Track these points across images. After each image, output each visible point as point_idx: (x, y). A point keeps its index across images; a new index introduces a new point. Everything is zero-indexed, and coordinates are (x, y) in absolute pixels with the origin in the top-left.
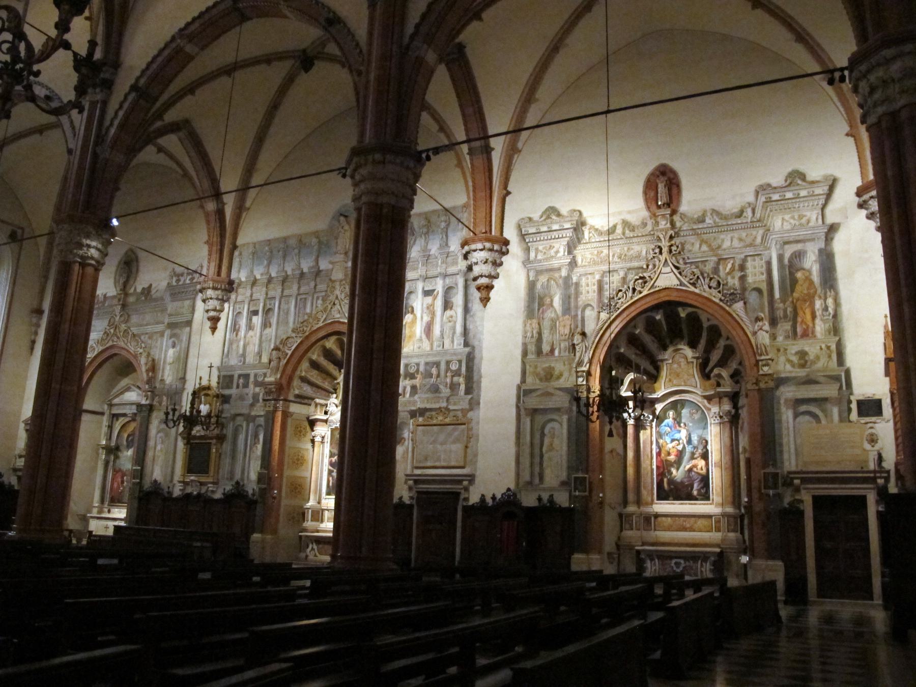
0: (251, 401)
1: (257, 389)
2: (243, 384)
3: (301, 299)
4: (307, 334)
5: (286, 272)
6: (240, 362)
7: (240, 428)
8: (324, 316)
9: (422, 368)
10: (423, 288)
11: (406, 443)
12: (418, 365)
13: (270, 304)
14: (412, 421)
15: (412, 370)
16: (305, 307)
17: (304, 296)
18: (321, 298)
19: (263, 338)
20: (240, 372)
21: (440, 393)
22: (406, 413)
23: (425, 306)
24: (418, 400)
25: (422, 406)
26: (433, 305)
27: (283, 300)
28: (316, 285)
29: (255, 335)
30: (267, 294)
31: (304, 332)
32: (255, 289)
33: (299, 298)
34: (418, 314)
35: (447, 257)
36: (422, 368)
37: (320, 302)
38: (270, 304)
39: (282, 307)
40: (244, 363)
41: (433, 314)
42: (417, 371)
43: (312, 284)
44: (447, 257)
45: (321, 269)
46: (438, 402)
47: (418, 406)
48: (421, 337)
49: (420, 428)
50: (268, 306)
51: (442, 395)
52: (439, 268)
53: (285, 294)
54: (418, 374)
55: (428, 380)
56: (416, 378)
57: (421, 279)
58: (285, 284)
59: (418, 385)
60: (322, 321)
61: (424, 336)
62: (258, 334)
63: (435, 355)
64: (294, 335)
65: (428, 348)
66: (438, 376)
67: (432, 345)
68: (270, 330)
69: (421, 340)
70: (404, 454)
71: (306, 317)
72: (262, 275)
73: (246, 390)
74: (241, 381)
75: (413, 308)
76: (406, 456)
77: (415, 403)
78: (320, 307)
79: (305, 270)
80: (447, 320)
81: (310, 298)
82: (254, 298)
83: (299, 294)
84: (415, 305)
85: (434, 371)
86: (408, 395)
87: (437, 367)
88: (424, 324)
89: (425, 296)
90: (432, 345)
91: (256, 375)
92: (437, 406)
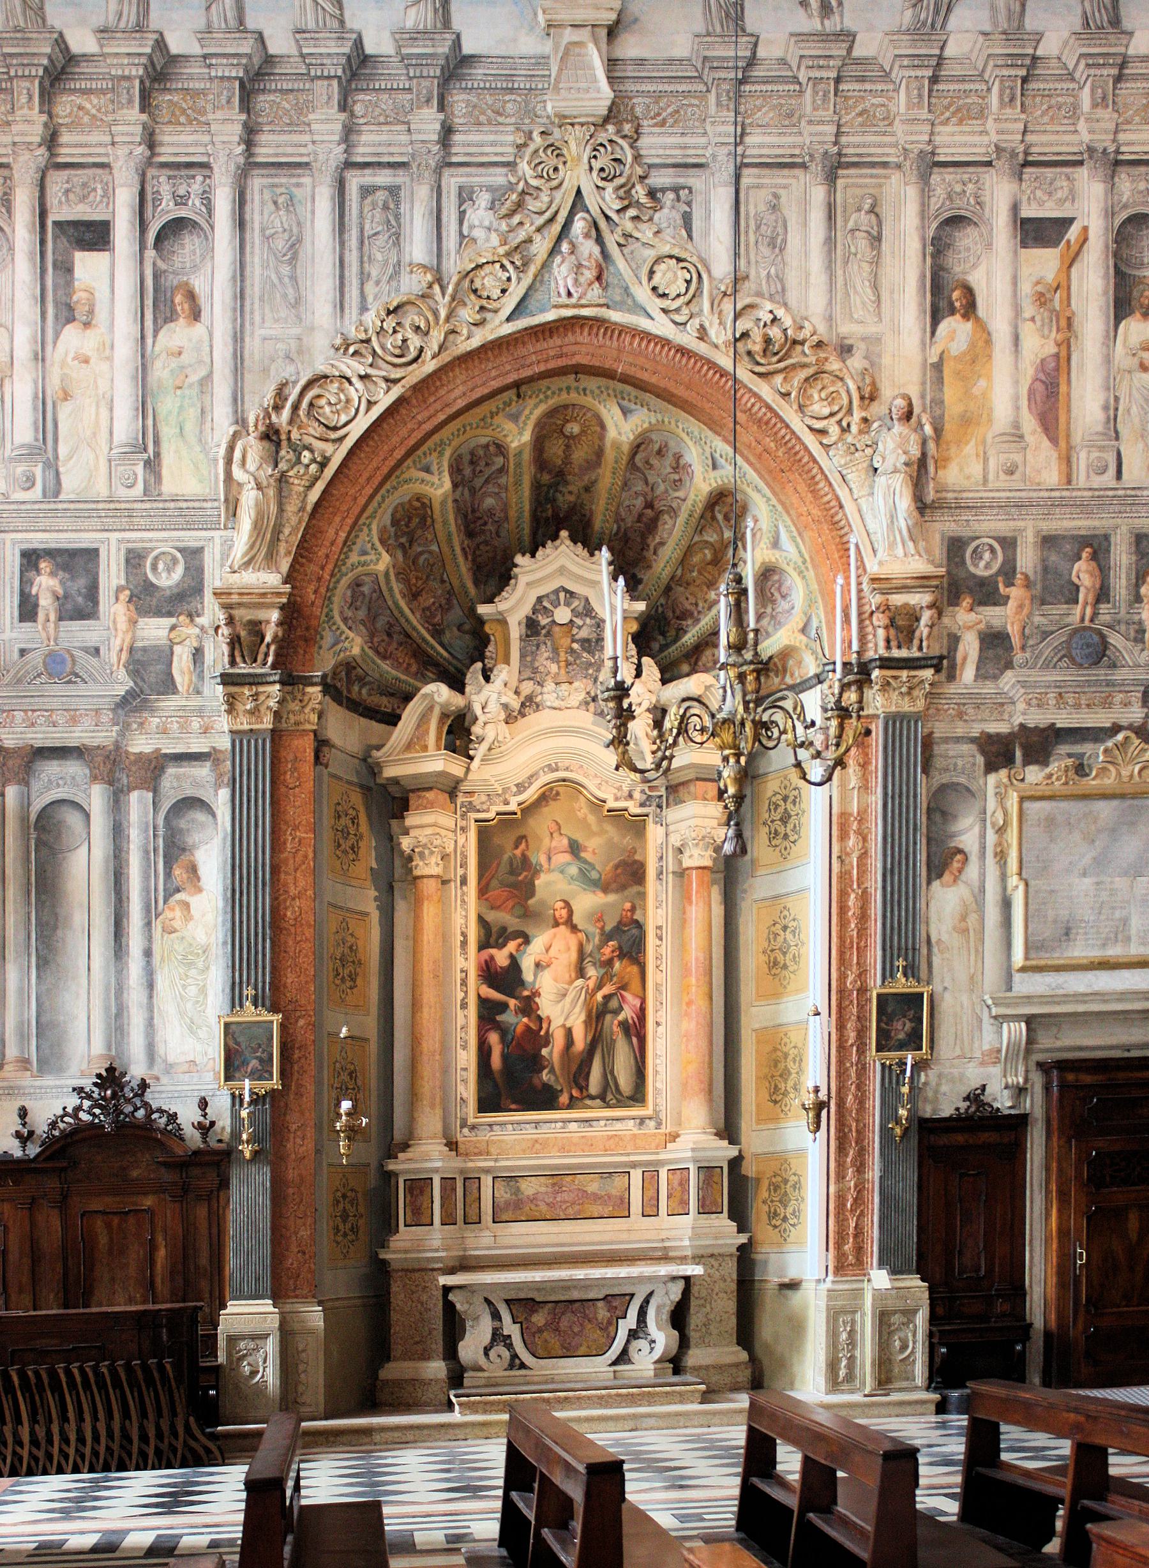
0: (123, 683)
1: (155, 630)
2: (62, 600)
3: (366, 191)
4: (429, 366)
5: (260, 38)
6: (30, 482)
7: (73, 819)
8: (516, 292)
9: (1027, 559)
10: (1015, 208)
11: (972, 871)
12: (1009, 543)
13: (181, 200)
14: (992, 779)
15: (983, 567)
16: (397, 239)
17: (383, 178)
18: (483, 199)
19: (160, 371)
20: (38, 540)
21: (1113, 666)
22: (967, 748)
23: (1026, 288)
24: (1018, 693)
25: (1037, 718)
26: (1063, 286)
27: (256, 183)
28: (447, 131)
29: (107, 349)
30: (151, 142)
31: (407, 358)
32: (65, 106)
33: (355, 181)
34: (1000, 325)
35: (1119, 79)
36: (1027, 559)
37: (479, 214)
38: (181, 200)
39: (256, 215)
40: (54, 489)
41: (1067, 325)
42: (1009, 572)
43: (428, 122)
44: (1119, 79)
45: (467, 49)
46: (1107, 703)
47: (1018, 720)
48: (1016, 425)
49: (1033, 807)
50: (166, 210)
51: (1120, 675)
52: (1082, 126)
53: (264, 153)
54: (1010, 584)
55: (1058, 610)
56: (1003, 601)
57: (1001, 164)
58: (262, 101)
59: (1013, 630)
60: (509, 304)
61: (1030, 424)
62: (124, 350)
63: (1084, 508)
64: (353, 367)
65: (1052, 476)
66: (1103, 594)
67: (1067, 461)
68: (199, 329)
69: (1017, 436)
70: (963, 918)
71: (412, 284)
72: (103, 32)
73: (79, 633)
74: (46, 584)
75: (969, 292)
76: (973, 919)
77: (1001, 705)
78: (489, 244)
79: (377, 43)
80: (1133, 363)
81: (423, 192)
82: (66, 154)
83: (349, 165)
84: (977, 279)
85: (1083, 573)
86: (968, 674)
87: (1094, 557)
88: (1029, 372)
89: (1024, 245)
90: (1067, 461)
91: (134, 559)
92: (1100, 719)
